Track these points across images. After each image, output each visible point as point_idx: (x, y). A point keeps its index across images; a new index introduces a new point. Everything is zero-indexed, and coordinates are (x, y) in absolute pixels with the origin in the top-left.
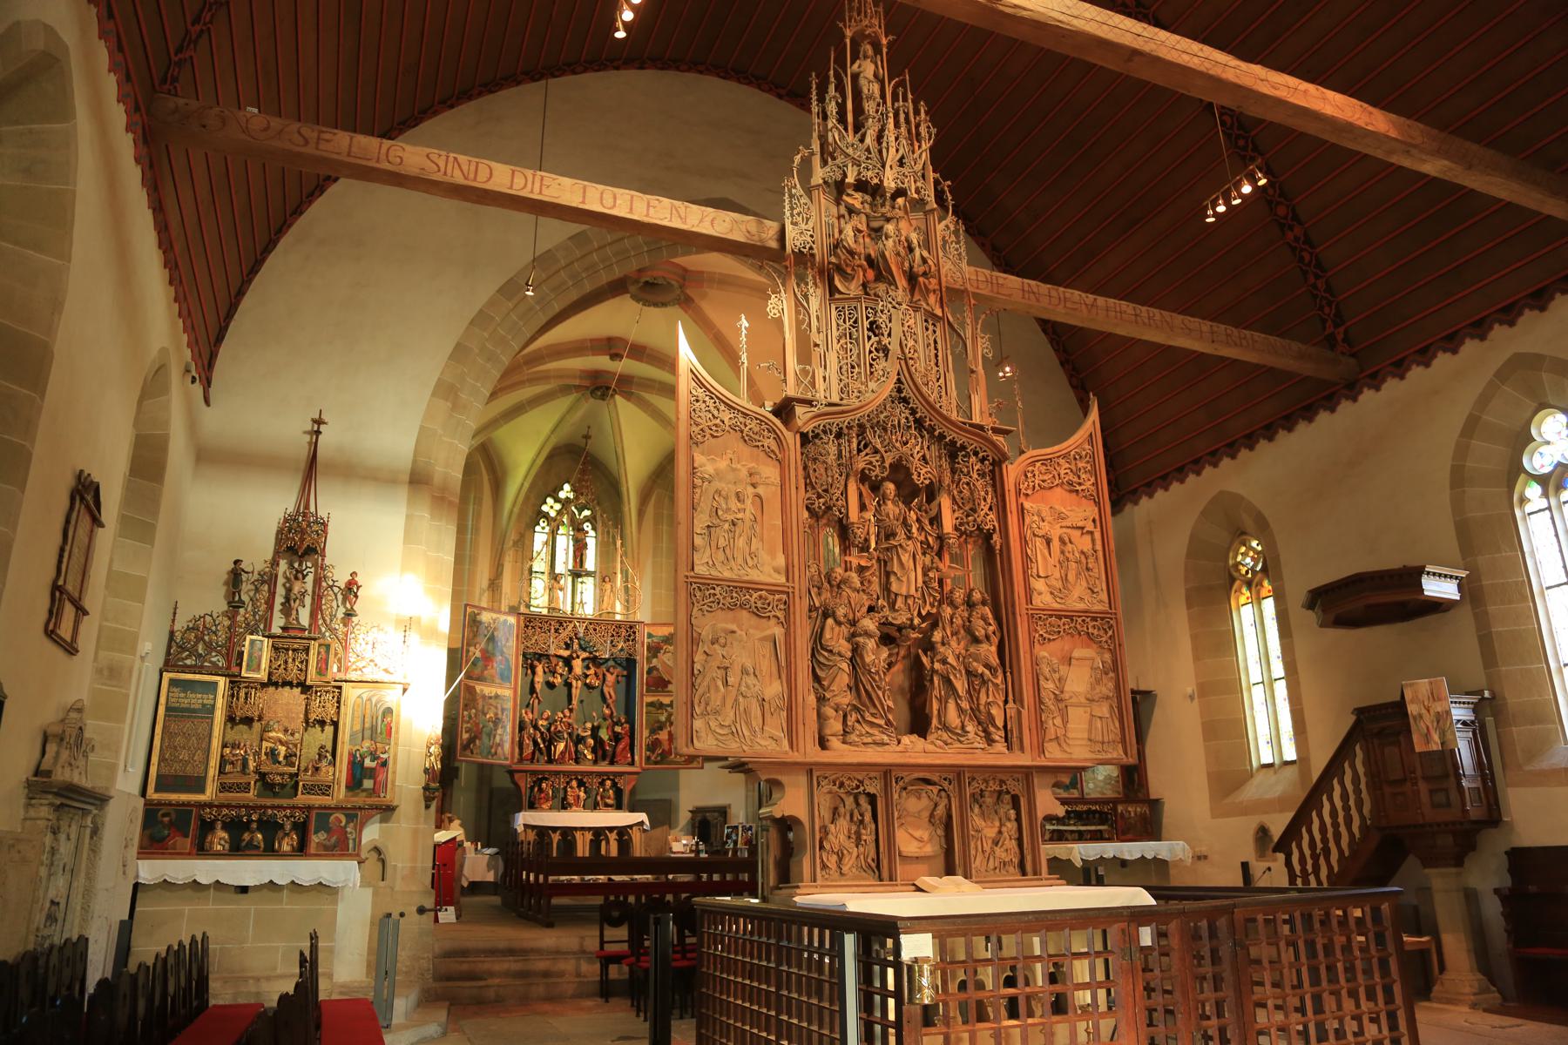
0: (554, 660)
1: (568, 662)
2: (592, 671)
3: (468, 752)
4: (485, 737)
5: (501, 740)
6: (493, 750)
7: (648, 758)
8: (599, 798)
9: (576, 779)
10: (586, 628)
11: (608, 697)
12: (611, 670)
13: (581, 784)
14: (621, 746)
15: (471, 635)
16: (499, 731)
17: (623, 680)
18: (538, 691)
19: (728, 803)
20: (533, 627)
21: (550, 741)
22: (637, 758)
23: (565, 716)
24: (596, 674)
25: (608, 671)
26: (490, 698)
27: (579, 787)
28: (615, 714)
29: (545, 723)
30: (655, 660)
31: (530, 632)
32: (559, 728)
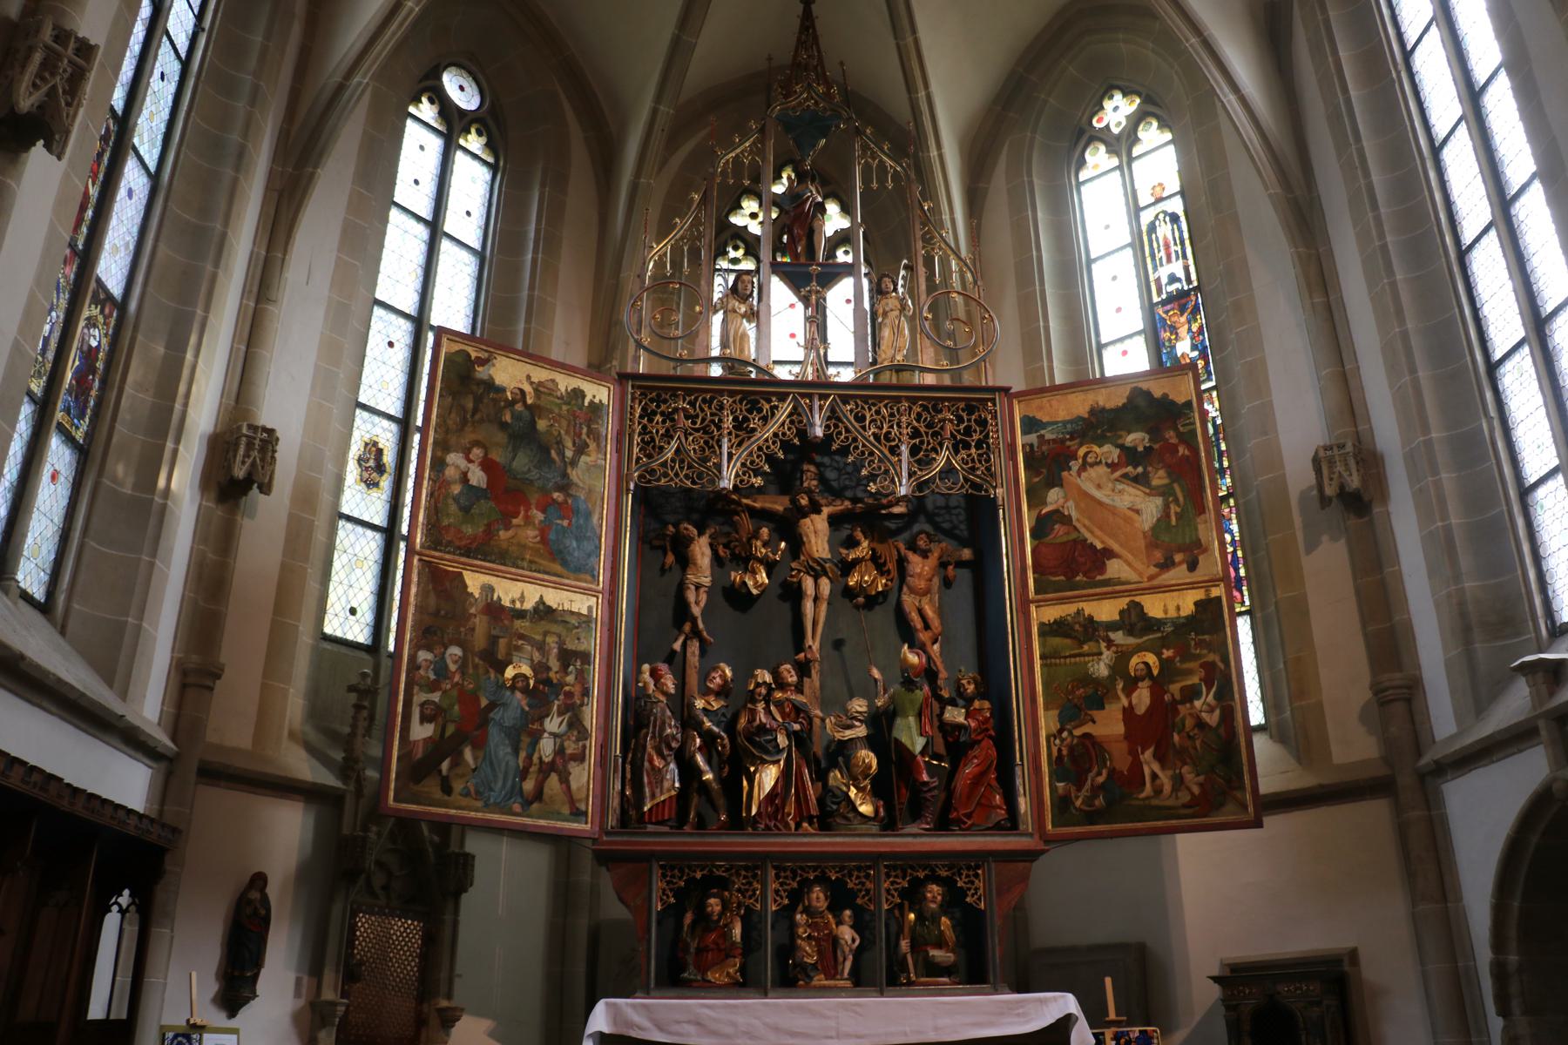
0: (746, 522)
1: (787, 528)
2: (864, 549)
3: (432, 787)
4: (495, 736)
5: (560, 751)
6: (529, 786)
7: (1063, 805)
8: (904, 945)
9: (822, 880)
10: (833, 417)
11: (919, 624)
12: (921, 543)
13: (840, 899)
14: (969, 770)
15: (454, 419)
16: (553, 724)
17: (964, 578)
18: (696, 611)
19: (1350, 944)
20: (668, 416)
21: (737, 768)
22: (1023, 804)
23: (781, 684)
24: (875, 559)
25: (912, 546)
26: (521, 614)
27: (835, 907)
28: (943, 674)
29: (716, 705)
30: (1054, 497)
31: (658, 425)
32: (762, 717)
